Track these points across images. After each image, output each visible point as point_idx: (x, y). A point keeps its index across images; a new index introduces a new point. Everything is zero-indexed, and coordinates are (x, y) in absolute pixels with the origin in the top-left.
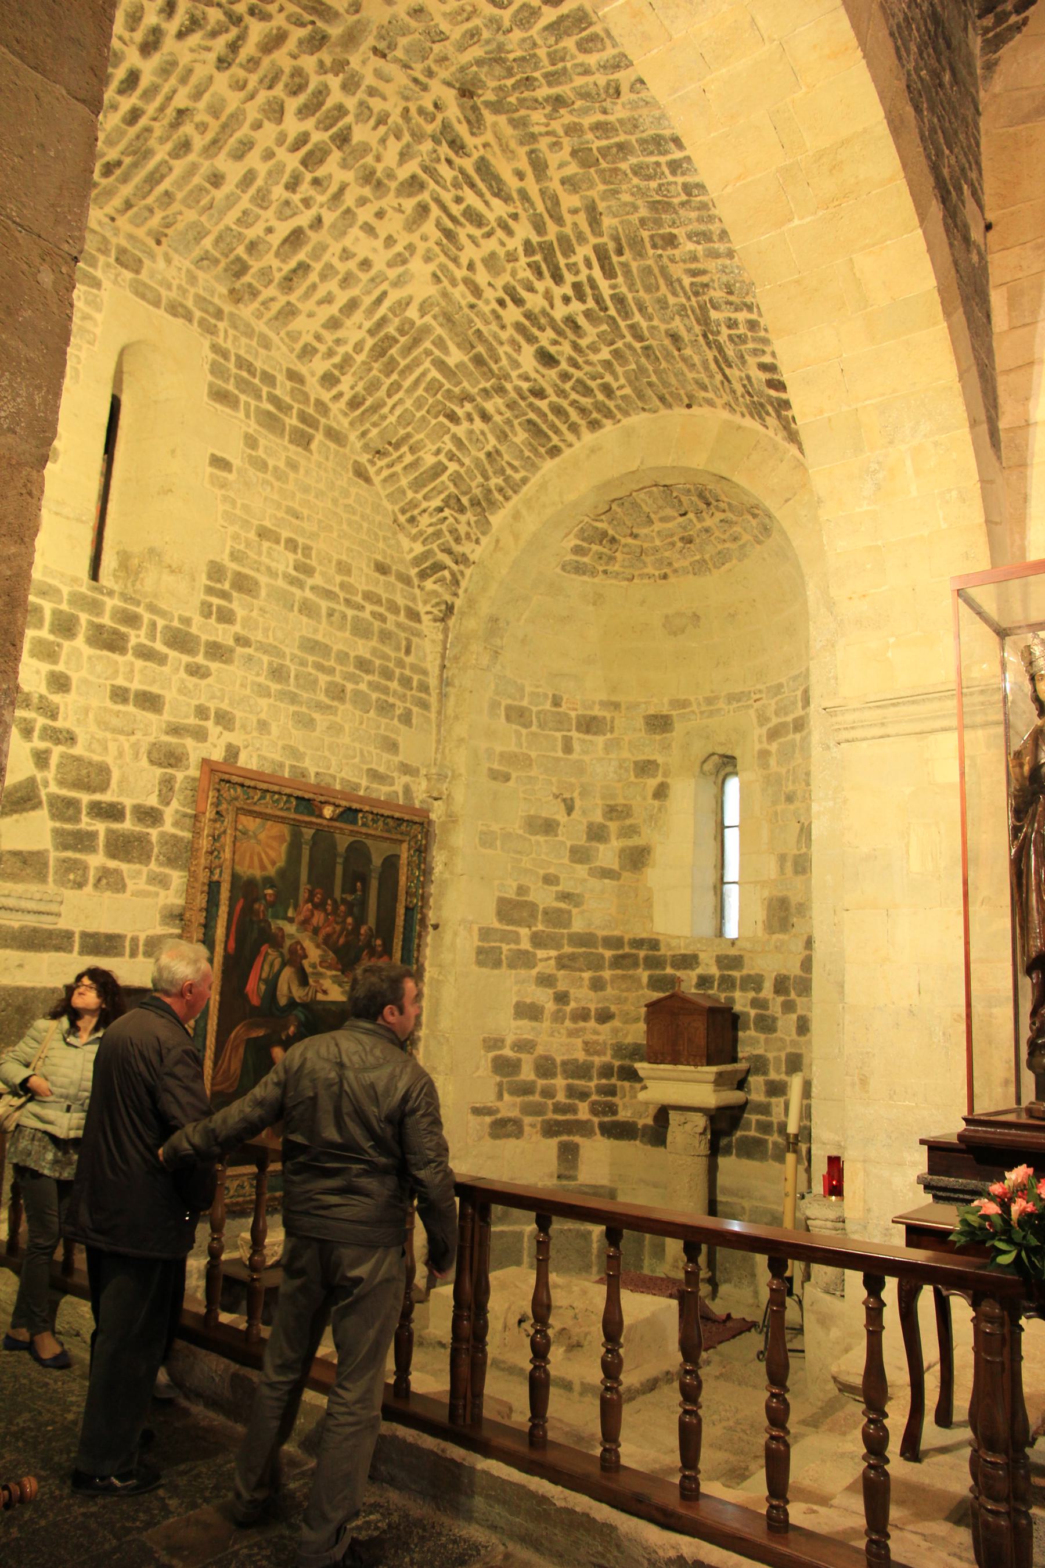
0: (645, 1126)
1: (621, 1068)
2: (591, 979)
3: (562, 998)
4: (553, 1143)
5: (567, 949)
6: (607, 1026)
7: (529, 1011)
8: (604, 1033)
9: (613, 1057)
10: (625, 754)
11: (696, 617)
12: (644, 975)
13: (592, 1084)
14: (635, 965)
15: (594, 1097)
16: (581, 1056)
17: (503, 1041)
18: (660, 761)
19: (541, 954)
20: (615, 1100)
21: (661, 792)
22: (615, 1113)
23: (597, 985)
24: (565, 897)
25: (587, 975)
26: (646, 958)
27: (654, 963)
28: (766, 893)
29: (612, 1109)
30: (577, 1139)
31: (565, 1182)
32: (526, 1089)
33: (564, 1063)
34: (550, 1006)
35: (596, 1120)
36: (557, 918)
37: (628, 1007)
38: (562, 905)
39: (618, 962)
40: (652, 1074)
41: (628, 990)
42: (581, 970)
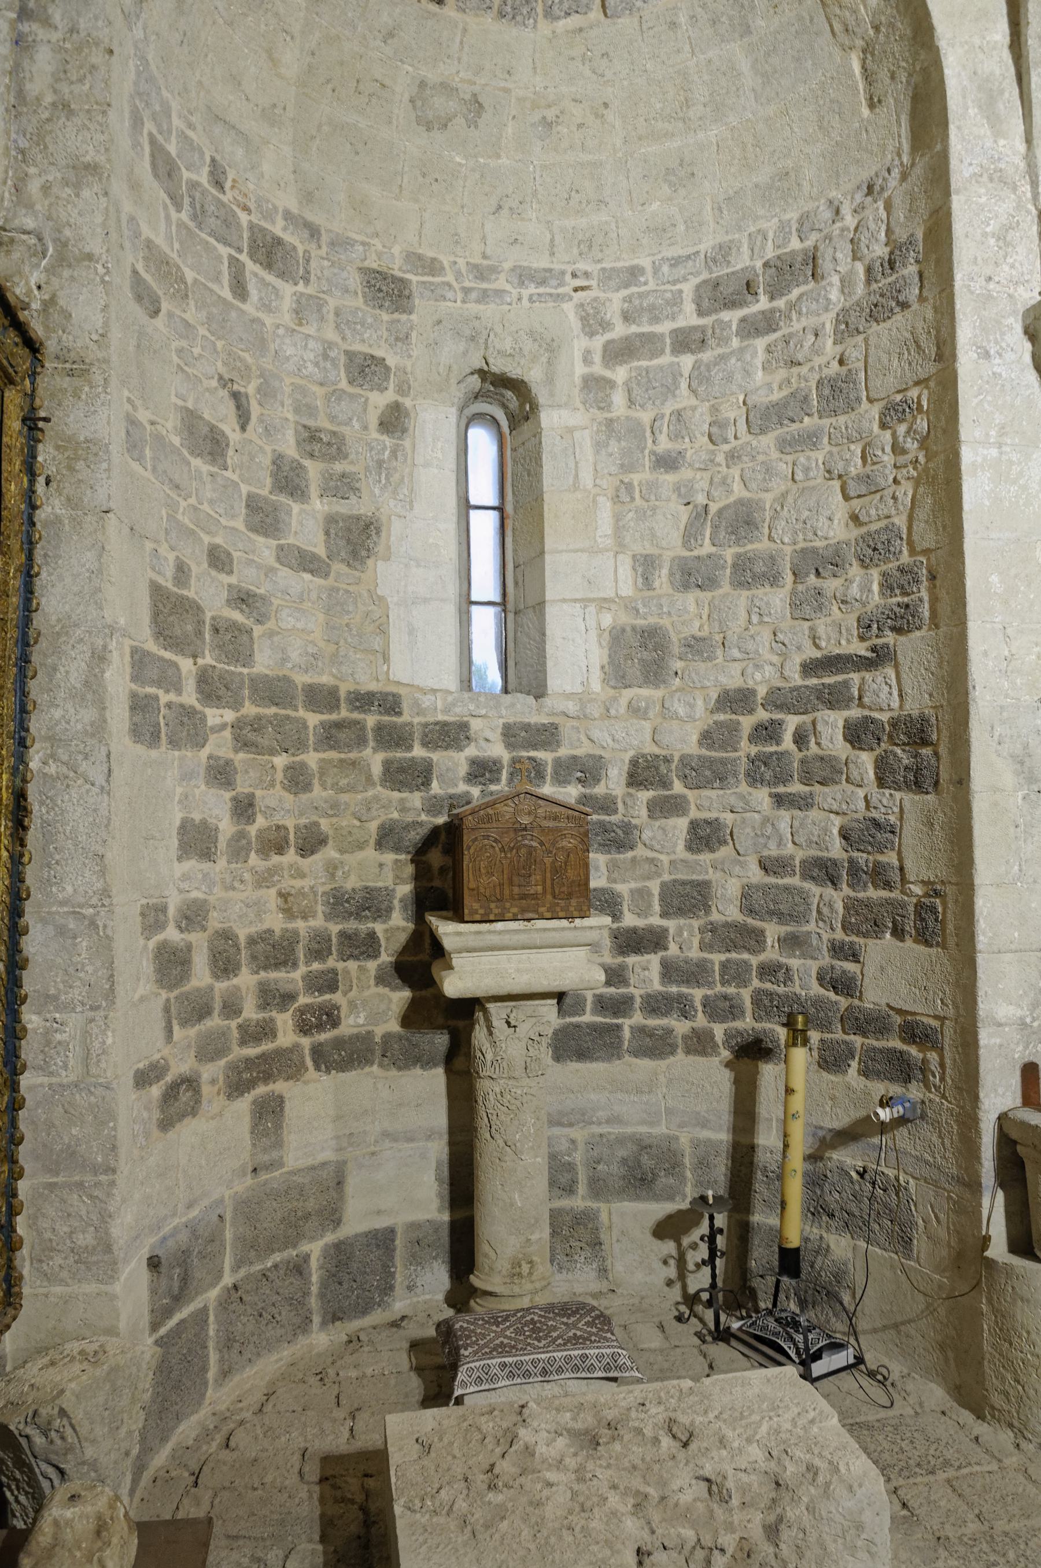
0: (387, 1037)
1: (342, 934)
2: (287, 768)
3: (244, 808)
4: (244, 1104)
5: (250, 709)
6: (318, 859)
7: (196, 840)
8: (311, 875)
9: (328, 917)
10: (331, 335)
11: (476, 105)
12: (375, 760)
13: (297, 975)
14: (361, 741)
15: (303, 1000)
16: (275, 922)
17: (164, 909)
18: (391, 361)
19: (214, 716)
20: (337, 998)
21: (394, 421)
22: (335, 1023)
23: (297, 780)
24: (243, 599)
25: (280, 761)
26: (379, 728)
27: (392, 737)
28: (607, 620)
29: (330, 1017)
30: (279, 1086)
31: (264, 1177)
32: (198, 1009)
33: (252, 941)
34: (226, 827)
35: (306, 1042)
36: (234, 642)
37: (347, 821)
38: (237, 616)
39: (330, 736)
40: (472, 942)
41: (350, 789)
42: (272, 752)
